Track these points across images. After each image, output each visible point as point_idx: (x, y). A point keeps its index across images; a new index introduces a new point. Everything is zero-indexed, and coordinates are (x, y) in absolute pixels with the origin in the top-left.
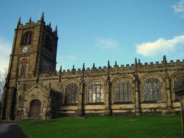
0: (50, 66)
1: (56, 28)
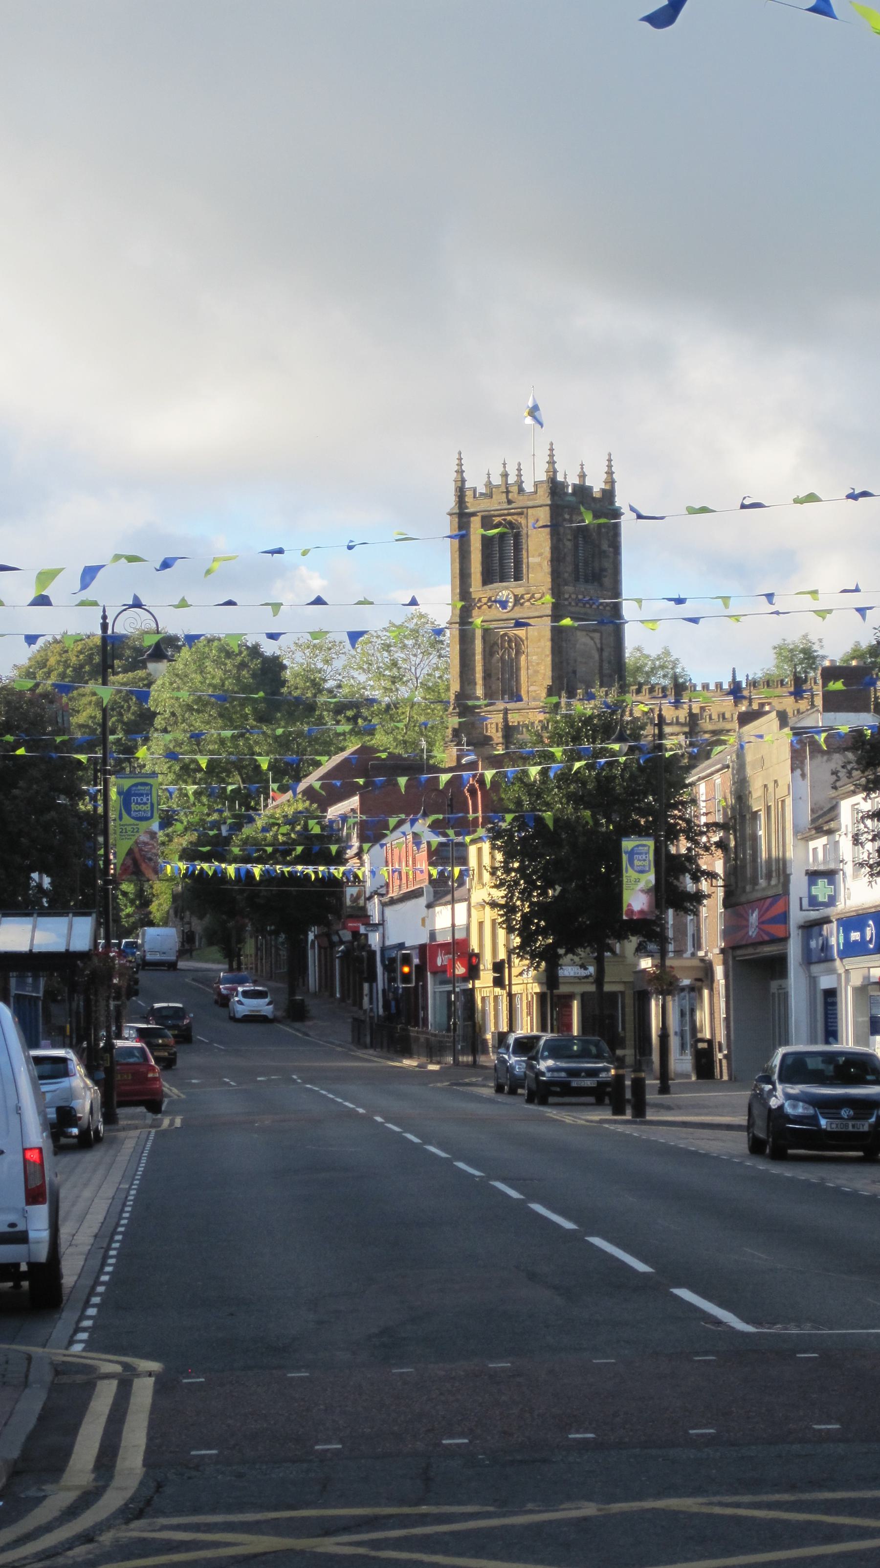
0: (601, 644)
1: (610, 466)
